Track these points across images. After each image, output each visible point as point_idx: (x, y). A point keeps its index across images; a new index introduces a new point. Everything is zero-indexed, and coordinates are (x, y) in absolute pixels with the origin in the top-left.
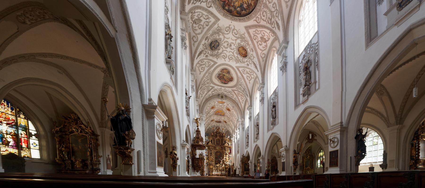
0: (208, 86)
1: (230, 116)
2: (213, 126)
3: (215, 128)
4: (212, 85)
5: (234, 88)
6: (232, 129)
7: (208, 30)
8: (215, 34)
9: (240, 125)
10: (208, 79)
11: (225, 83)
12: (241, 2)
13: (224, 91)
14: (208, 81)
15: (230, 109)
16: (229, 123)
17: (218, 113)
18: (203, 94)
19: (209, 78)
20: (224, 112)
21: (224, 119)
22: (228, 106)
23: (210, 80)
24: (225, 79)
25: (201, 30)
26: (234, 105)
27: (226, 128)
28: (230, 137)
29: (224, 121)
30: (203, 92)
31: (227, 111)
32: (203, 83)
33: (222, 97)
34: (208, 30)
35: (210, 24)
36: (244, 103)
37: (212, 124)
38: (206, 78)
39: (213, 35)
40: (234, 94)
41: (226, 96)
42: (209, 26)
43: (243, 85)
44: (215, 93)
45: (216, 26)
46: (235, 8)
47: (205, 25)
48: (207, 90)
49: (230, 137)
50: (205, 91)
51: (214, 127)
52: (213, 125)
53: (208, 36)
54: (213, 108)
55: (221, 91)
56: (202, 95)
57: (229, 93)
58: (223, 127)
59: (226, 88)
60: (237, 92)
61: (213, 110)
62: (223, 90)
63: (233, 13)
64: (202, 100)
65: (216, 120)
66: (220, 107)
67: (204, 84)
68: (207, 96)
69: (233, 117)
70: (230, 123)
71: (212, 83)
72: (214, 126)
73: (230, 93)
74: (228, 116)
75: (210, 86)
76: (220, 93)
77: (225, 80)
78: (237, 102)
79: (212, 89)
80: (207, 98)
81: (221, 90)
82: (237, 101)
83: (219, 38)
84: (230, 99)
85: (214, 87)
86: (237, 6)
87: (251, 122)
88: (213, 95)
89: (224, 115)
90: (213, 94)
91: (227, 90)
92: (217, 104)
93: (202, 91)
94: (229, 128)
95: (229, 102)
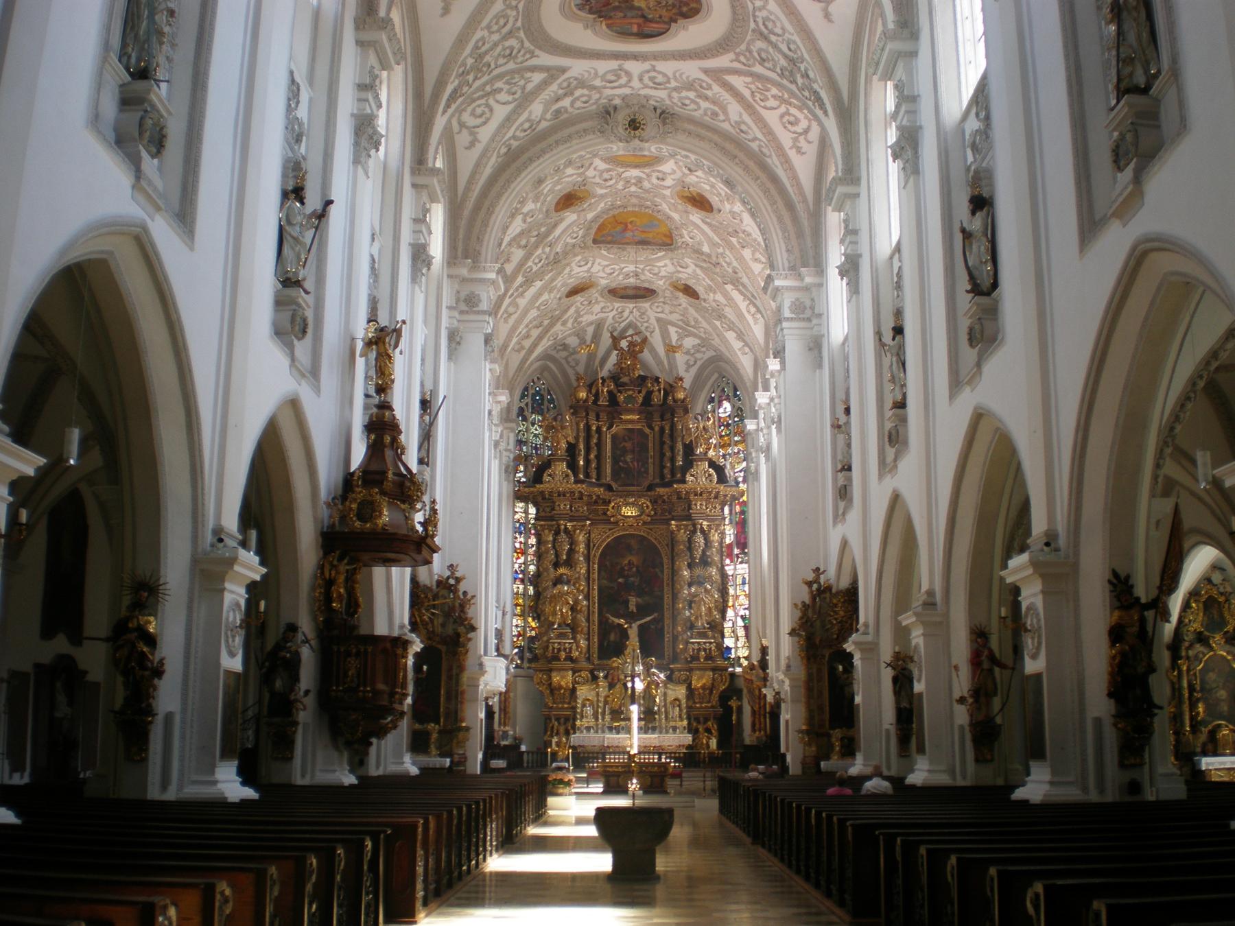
0: (513, 72)
1: (716, 245)
2: (590, 330)
3: (606, 340)
4: (546, 59)
5: (713, 56)
6: (747, 344)
9: (788, 319)
10: (505, 30)
11: (644, 36)
13: (646, 80)
14: (512, 42)
15: (708, 196)
16: (719, 297)
17: (619, 228)
18: (485, 123)
19: (519, 24)
20: (669, 217)
21: (671, 268)
22: (692, 179)
23: (522, 34)
24: (640, 9)
26: (736, 172)
27: (695, 335)
28: (739, 413)
29: (676, 288)
30: (479, 111)
31: (690, 207)
32: (470, 61)
33: (634, 125)
36: (811, 150)
37: (577, 312)
38: (495, 28)
40: (726, 96)
41: (665, 116)
43: (778, 35)
44: (578, 104)
48: (510, 98)
49: (739, 413)
50: (497, 101)
51: (596, 337)
52: (593, 318)
54: (569, 200)
55: (620, 87)
56: (473, 134)
57: (684, 94)
58: (672, 330)
59: (654, 63)
60: (742, 78)
61: (573, 217)
62: (641, 80)
64: (478, 165)
65: (613, 285)
66: (633, 189)
67: (480, 66)
68: (514, 137)
69: (747, 253)
70: (726, 295)
71: (540, 48)
72: (599, 325)
73: (692, 95)
74: (706, 249)
75: (533, 69)
76: (617, 101)
77: (643, 16)
78: (754, 145)
79: (545, 84)
80: (515, 144)
81: (623, 80)
82: (755, 139)
84: (703, 132)
85: (563, 70)
87: (858, 302)
88: (566, 116)
89: (667, 242)
90: (558, 112)
91: (665, 75)
92: (606, 176)
93: (469, 109)
94: (725, 341)
95: (693, 157)
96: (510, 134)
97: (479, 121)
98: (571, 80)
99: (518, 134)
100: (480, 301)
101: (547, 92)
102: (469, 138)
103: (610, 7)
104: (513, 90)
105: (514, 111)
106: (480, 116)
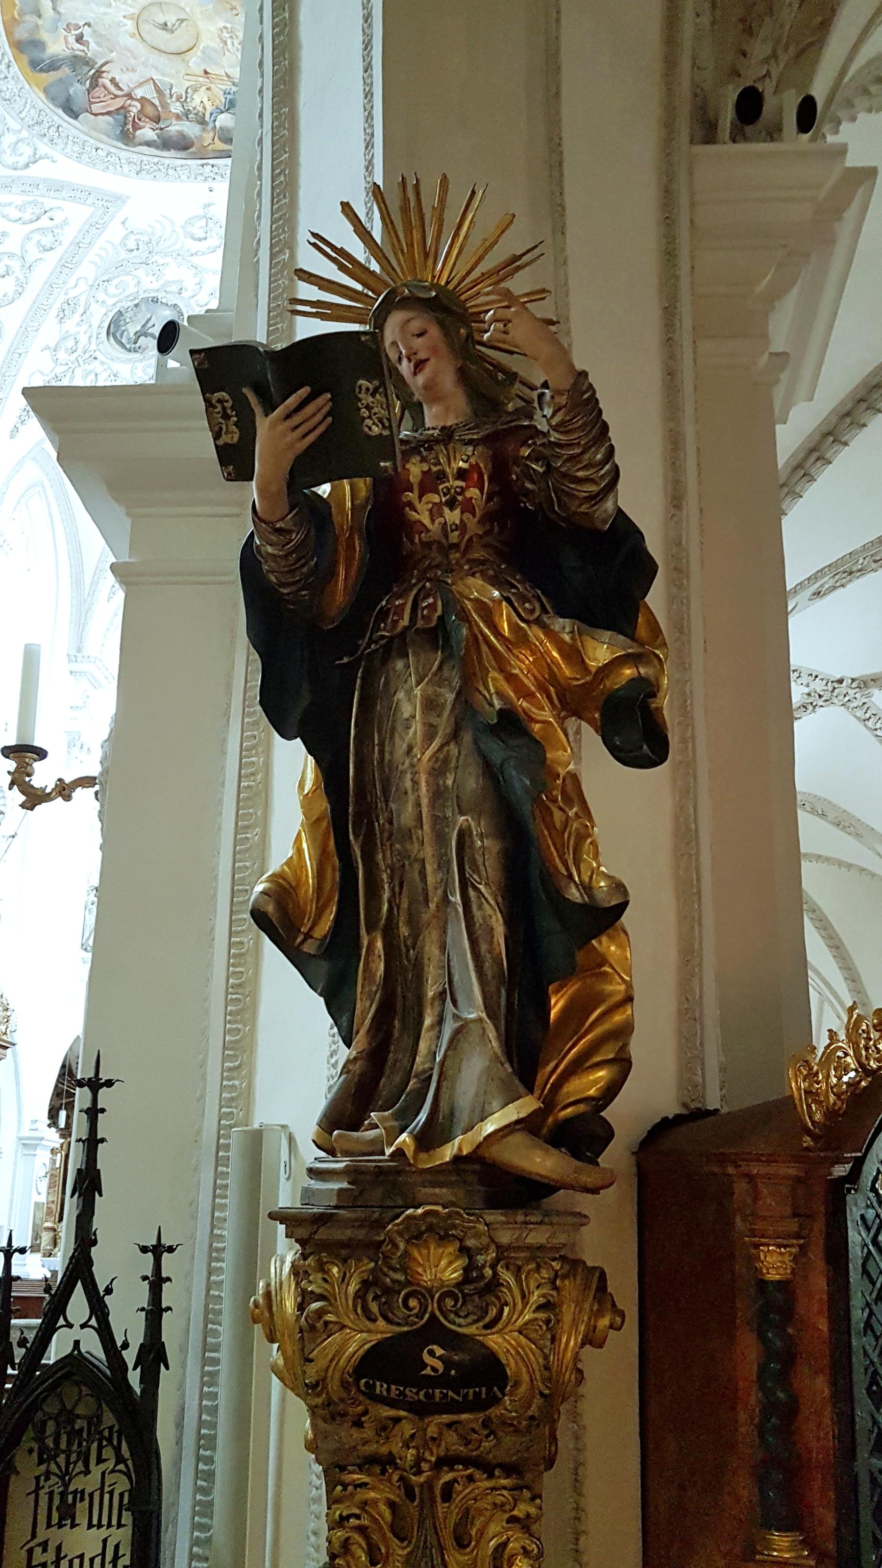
7: (66, 265)
8: (128, 273)
12: (223, 87)
25: (18, 279)
34: (66, 265)
35: (68, 236)
39: (115, 282)
42: (59, 251)
45: (114, 232)
46: (202, 122)
47: (31, 247)
53: (72, 294)
63: (196, 144)
83: (163, 285)
86: (210, 108)
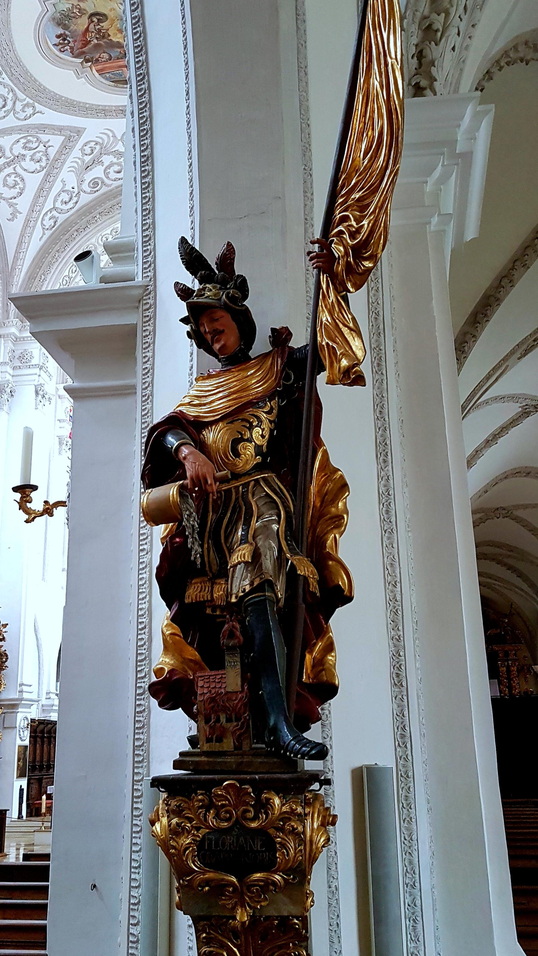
30: (11, 181)
56: (11, 205)
85: (79, 132)
88: (104, 189)
90: (95, 183)
96: (49, 205)
97: (14, 192)
98: (92, 144)
99: (58, 205)
100: (32, 357)
101: (70, 159)
102: (11, 210)
103: (90, 46)
104: (38, 156)
105: (45, 180)
106: (14, 187)
